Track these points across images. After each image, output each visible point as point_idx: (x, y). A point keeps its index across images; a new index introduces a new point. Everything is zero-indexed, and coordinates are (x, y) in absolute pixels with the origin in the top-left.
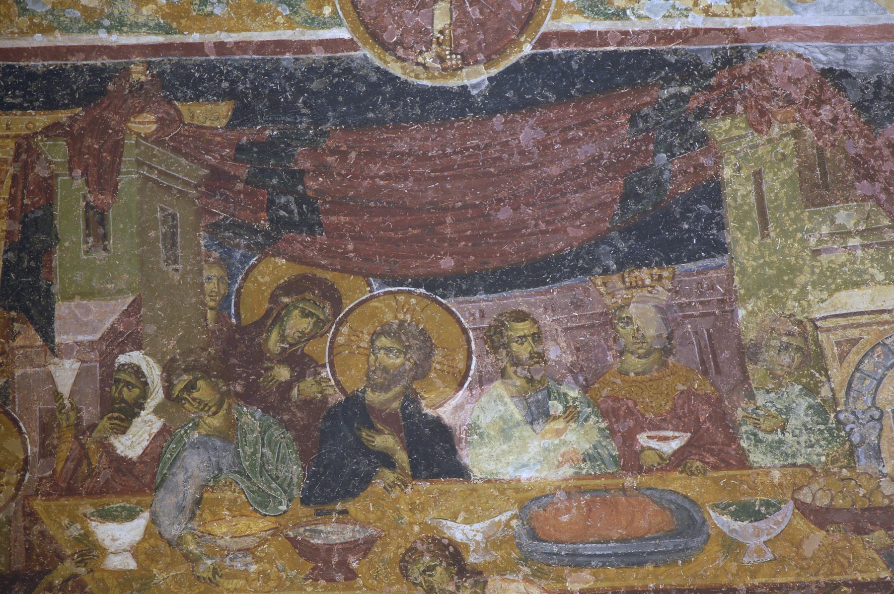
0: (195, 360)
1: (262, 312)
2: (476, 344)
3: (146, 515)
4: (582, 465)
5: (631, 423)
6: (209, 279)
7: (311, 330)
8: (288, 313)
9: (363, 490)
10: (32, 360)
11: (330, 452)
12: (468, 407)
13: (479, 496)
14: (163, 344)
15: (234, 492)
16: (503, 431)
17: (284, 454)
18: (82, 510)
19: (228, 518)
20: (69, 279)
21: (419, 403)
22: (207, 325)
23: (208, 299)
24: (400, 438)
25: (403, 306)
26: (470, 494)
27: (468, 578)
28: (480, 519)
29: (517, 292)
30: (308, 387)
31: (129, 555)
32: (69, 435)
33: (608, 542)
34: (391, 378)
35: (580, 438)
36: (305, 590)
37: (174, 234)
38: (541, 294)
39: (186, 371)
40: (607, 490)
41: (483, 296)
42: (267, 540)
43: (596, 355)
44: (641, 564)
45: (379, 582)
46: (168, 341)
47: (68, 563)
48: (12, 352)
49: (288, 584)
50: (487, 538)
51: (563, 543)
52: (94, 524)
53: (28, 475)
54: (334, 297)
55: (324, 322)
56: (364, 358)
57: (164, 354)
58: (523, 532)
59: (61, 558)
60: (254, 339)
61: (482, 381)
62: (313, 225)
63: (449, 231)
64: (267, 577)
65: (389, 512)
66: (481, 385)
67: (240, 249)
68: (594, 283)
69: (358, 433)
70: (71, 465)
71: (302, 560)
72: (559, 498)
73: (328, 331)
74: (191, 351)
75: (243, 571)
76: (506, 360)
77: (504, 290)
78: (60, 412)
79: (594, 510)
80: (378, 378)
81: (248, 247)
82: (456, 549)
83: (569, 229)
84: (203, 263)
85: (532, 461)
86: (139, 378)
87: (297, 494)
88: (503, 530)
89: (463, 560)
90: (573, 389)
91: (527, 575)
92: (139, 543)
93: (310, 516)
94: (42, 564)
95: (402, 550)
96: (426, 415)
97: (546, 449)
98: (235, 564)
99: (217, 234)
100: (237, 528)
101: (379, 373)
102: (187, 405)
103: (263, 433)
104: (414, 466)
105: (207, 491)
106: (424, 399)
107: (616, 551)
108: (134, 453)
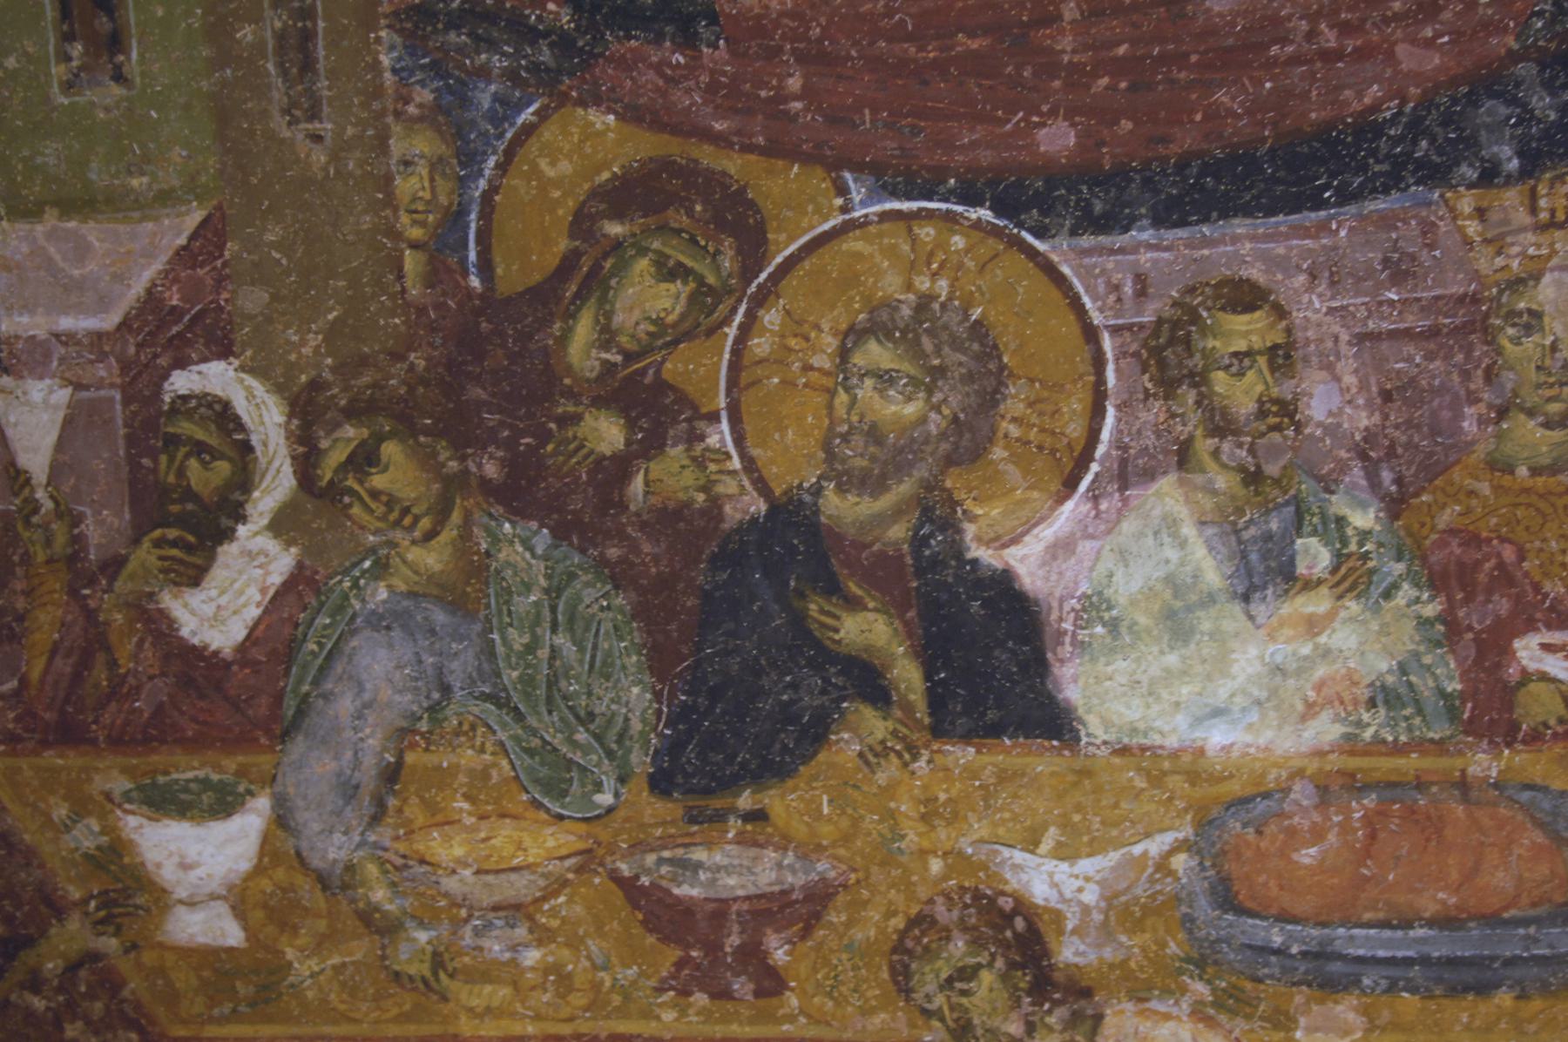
0: (375, 385)
1: (552, 262)
2: (1117, 370)
4: (1366, 717)
5: (1503, 606)
6: (407, 163)
7: (683, 316)
8: (622, 267)
9: (806, 759)
12: (1086, 547)
13: (1098, 790)
14: (288, 342)
15: (482, 750)
16: (1169, 615)
17: (609, 654)
18: (99, 784)
19: (469, 821)
21: (960, 531)
22: (404, 291)
23: (405, 219)
24: (906, 624)
25: (931, 254)
26: (1075, 784)
27: (1056, 1003)
28: (1096, 848)
29: (1240, 226)
30: (669, 475)
31: (222, 908)
32: (55, 585)
33: (1407, 925)
34: (890, 455)
35: (1364, 641)
36: (658, 1018)
37: (307, 36)
38: (1304, 232)
39: (352, 413)
40: (1420, 785)
41: (1147, 235)
42: (565, 883)
43: (1434, 414)
44: (1484, 989)
45: (837, 1003)
47: (74, 924)
49: (617, 1000)
50: (1110, 898)
51: (1295, 920)
52: (132, 821)
55: (717, 294)
58: (1200, 887)
59: (59, 910)
60: (531, 337)
61: (1129, 474)
63: (1066, 43)
64: (565, 982)
65: (871, 821)
66: (1123, 488)
67: (489, 82)
68: (1452, 210)
69: (796, 604)
70: (64, 666)
71: (651, 940)
72: (1297, 803)
73: (727, 321)
74: (364, 362)
75: (504, 964)
76: (1194, 417)
77: (1206, 219)
78: (27, 523)
79: (1382, 835)
80: (855, 456)
81: (512, 75)
83: (1401, 50)
84: (390, 119)
85: (1237, 700)
86: (229, 434)
87: (640, 761)
88: (1151, 881)
89: (1046, 954)
90: (1363, 506)
91: (1201, 1002)
93: (673, 822)
95: (898, 922)
97: (1279, 670)
98: (486, 943)
99: (425, 38)
100: (492, 848)
101: (858, 440)
102: (356, 510)
103: (554, 592)
104: (937, 699)
105: (413, 746)
106: (973, 519)
107: (1426, 949)
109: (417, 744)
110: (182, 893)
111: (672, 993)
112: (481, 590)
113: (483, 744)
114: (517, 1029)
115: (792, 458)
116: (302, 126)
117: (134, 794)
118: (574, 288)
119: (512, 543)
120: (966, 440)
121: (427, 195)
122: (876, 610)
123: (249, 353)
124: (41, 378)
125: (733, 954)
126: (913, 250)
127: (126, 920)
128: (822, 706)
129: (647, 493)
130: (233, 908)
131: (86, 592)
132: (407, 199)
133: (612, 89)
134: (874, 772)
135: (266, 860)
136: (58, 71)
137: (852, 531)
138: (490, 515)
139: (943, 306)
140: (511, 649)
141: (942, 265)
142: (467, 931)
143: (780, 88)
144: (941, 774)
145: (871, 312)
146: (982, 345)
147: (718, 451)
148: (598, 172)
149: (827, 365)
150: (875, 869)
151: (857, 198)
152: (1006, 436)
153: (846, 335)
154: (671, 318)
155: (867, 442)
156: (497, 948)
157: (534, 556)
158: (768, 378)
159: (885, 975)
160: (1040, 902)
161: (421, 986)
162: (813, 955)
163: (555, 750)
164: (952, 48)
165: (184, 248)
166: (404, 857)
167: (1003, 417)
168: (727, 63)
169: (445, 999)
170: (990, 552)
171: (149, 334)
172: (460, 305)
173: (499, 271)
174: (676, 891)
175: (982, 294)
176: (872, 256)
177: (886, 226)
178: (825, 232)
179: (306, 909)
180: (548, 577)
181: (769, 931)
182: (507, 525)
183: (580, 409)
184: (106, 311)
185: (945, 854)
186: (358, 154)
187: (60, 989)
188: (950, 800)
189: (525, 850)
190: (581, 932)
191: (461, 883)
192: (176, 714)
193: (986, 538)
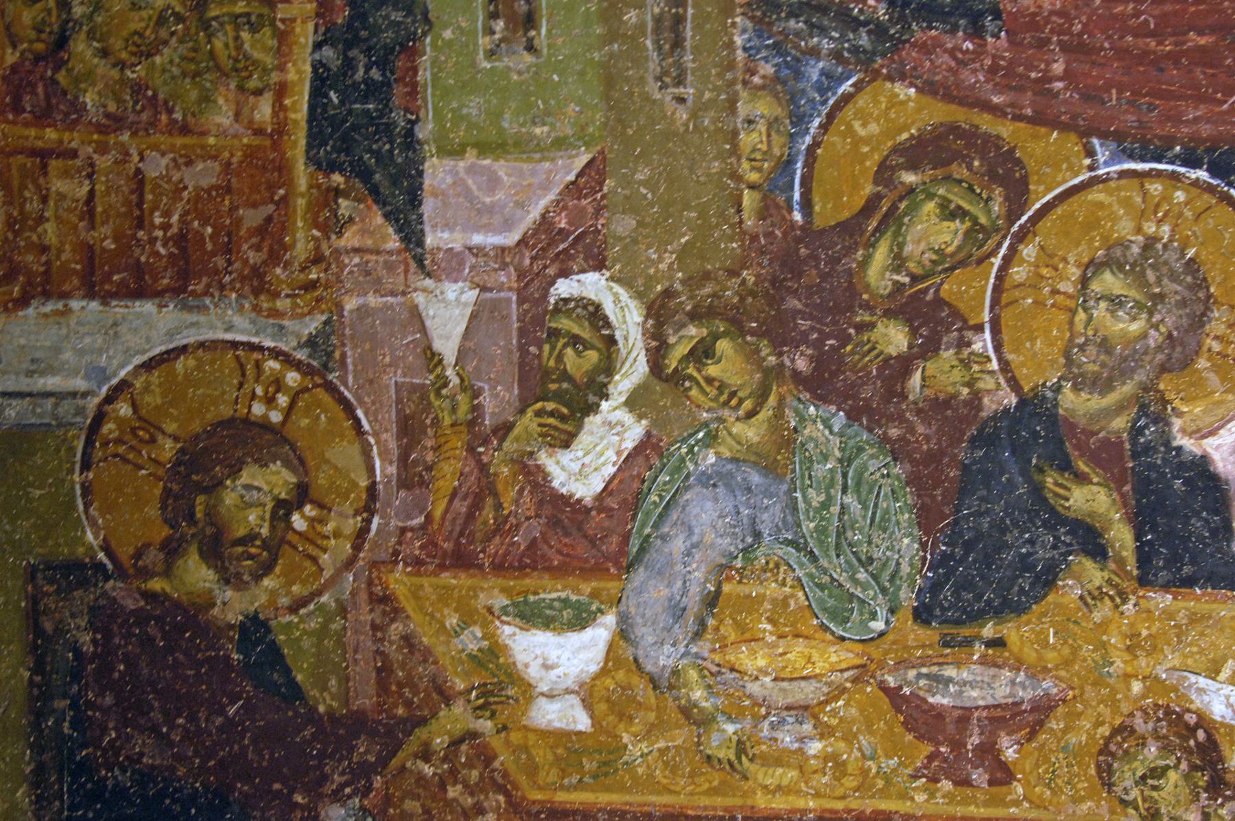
0: (714, 295)
1: (860, 203)
3: (610, 619)
6: (750, 122)
7: (959, 248)
8: (914, 208)
9: (1038, 600)
10: (379, 281)
11: (979, 514)
14: (649, 259)
15: (784, 584)
17: (887, 511)
18: (483, 599)
19: (771, 639)
20: (453, 111)
21: (1168, 424)
22: (741, 222)
23: (745, 165)
24: (1123, 496)
25: (1158, 206)
30: (942, 372)
31: (575, 700)
32: (458, 443)
34: (1119, 362)
36: (912, 799)
37: (679, 20)
39: (694, 316)
46: (661, 252)
47: (458, 708)
48: (337, 259)
49: (880, 783)
52: (508, 630)
53: (376, 521)
54: (1011, 178)
56: (1063, 317)
57: (650, 281)
59: (447, 698)
60: (840, 260)
62: (981, 14)
64: (840, 768)
67: (818, 60)
69: (1037, 477)
70: (461, 507)
71: (909, 737)
73: (993, 253)
74: (707, 276)
80: (1089, 362)
81: (837, 55)
82: (1209, 736)
84: (739, 87)
86: (598, 329)
87: (908, 599)
89: (1221, 760)
92: (596, 677)
93: (931, 646)
94: (408, 704)
95: (1105, 730)
96: (1179, 449)
98: (779, 735)
99: (770, 24)
101: (1092, 350)
102: (694, 392)
103: (845, 462)
104: (1144, 556)
105: (729, 579)
106: (1180, 415)
108: (587, 489)
109: (733, 577)
110: (544, 688)
111: (924, 780)
112: (788, 458)
113: (784, 579)
114: (801, 803)
115: (1039, 365)
116: (669, 90)
117: (511, 609)
118: (875, 224)
119: (815, 422)
120: (1177, 354)
121: (764, 147)
122: (1098, 484)
123: (617, 267)
124: (456, 281)
125: (973, 751)
126: (1144, 202)
127: (499, 707)
128: (1053, 558)
129: (923, 386)
130: (583, 701)
131: (481, 449)
132: (748, 150)
133: (914, 68)
134: (1091, 612)
135: (610, 664)
136: (484, 42)
137: (1084, 421)
138: (799, 399)
139: (1165, 246)
140: (810, 506)
141: (1165, 215)
142: (766, 725)
143: (1046, 71)
144: (1144, 615)
145: (1108, 249)
146: (1194, 278)
147: (981, 355)
148: (900, 132)
149: (1071, 291)
150: (1088, 688)
151: (1101, 159)
152: (1209, 350)
153: (1087, 267)
154: (950, 250)
155: (1099, 352)
156: (788, 739)
157: (831, 432)
158: (1024, 298)
159: (1093, 771)
160: (1219, 719)
161: (728, 767)
162: (1036, 753)
163: (840, 585)
164: (1184, 43)
165: (573, 183)
166: (718, 665)
167: (1208, 335)
168: (1006, 51)
169: (746, 778)
170: (1192, 441)
171: (542, 249)
172: (785, 234)
173: (817, 208)
174: (931, 700)
175: (1197, 238)
176: (1110, 205)
177: (1123, 182)
178: (1075, 186)
179: (640, 704)
180: (842, 450)
181: (1002, 734)
182: (812, 408)
183: (875, 318)
184: (510, 231)
185: (1144, 678)
186: (712, 114)
187: (445, 759)
188: (1150, 635)
189: (814, 663)
190: (855, 729)
191: (761, 688)
192: (545, 547)
193: (1189, 430)
